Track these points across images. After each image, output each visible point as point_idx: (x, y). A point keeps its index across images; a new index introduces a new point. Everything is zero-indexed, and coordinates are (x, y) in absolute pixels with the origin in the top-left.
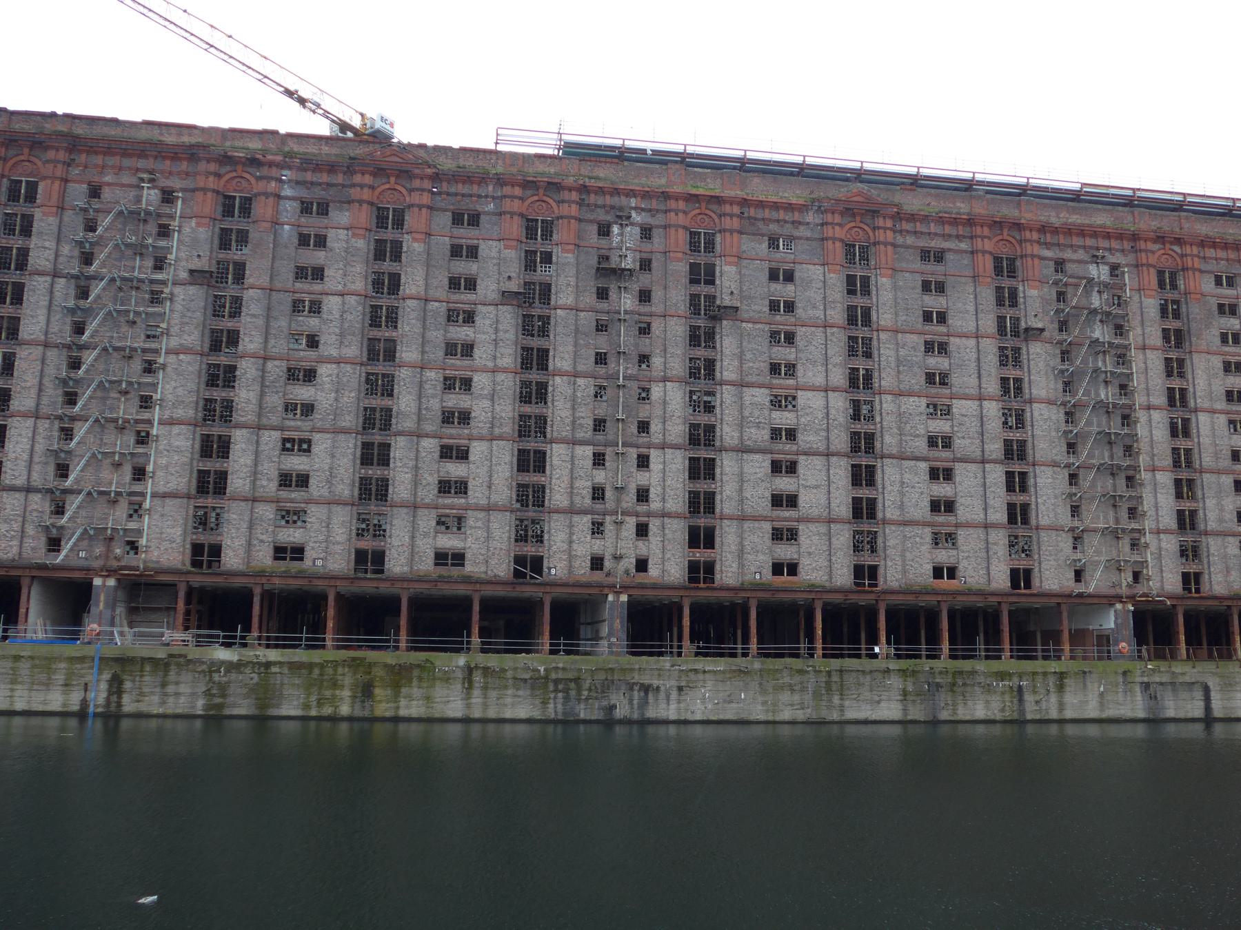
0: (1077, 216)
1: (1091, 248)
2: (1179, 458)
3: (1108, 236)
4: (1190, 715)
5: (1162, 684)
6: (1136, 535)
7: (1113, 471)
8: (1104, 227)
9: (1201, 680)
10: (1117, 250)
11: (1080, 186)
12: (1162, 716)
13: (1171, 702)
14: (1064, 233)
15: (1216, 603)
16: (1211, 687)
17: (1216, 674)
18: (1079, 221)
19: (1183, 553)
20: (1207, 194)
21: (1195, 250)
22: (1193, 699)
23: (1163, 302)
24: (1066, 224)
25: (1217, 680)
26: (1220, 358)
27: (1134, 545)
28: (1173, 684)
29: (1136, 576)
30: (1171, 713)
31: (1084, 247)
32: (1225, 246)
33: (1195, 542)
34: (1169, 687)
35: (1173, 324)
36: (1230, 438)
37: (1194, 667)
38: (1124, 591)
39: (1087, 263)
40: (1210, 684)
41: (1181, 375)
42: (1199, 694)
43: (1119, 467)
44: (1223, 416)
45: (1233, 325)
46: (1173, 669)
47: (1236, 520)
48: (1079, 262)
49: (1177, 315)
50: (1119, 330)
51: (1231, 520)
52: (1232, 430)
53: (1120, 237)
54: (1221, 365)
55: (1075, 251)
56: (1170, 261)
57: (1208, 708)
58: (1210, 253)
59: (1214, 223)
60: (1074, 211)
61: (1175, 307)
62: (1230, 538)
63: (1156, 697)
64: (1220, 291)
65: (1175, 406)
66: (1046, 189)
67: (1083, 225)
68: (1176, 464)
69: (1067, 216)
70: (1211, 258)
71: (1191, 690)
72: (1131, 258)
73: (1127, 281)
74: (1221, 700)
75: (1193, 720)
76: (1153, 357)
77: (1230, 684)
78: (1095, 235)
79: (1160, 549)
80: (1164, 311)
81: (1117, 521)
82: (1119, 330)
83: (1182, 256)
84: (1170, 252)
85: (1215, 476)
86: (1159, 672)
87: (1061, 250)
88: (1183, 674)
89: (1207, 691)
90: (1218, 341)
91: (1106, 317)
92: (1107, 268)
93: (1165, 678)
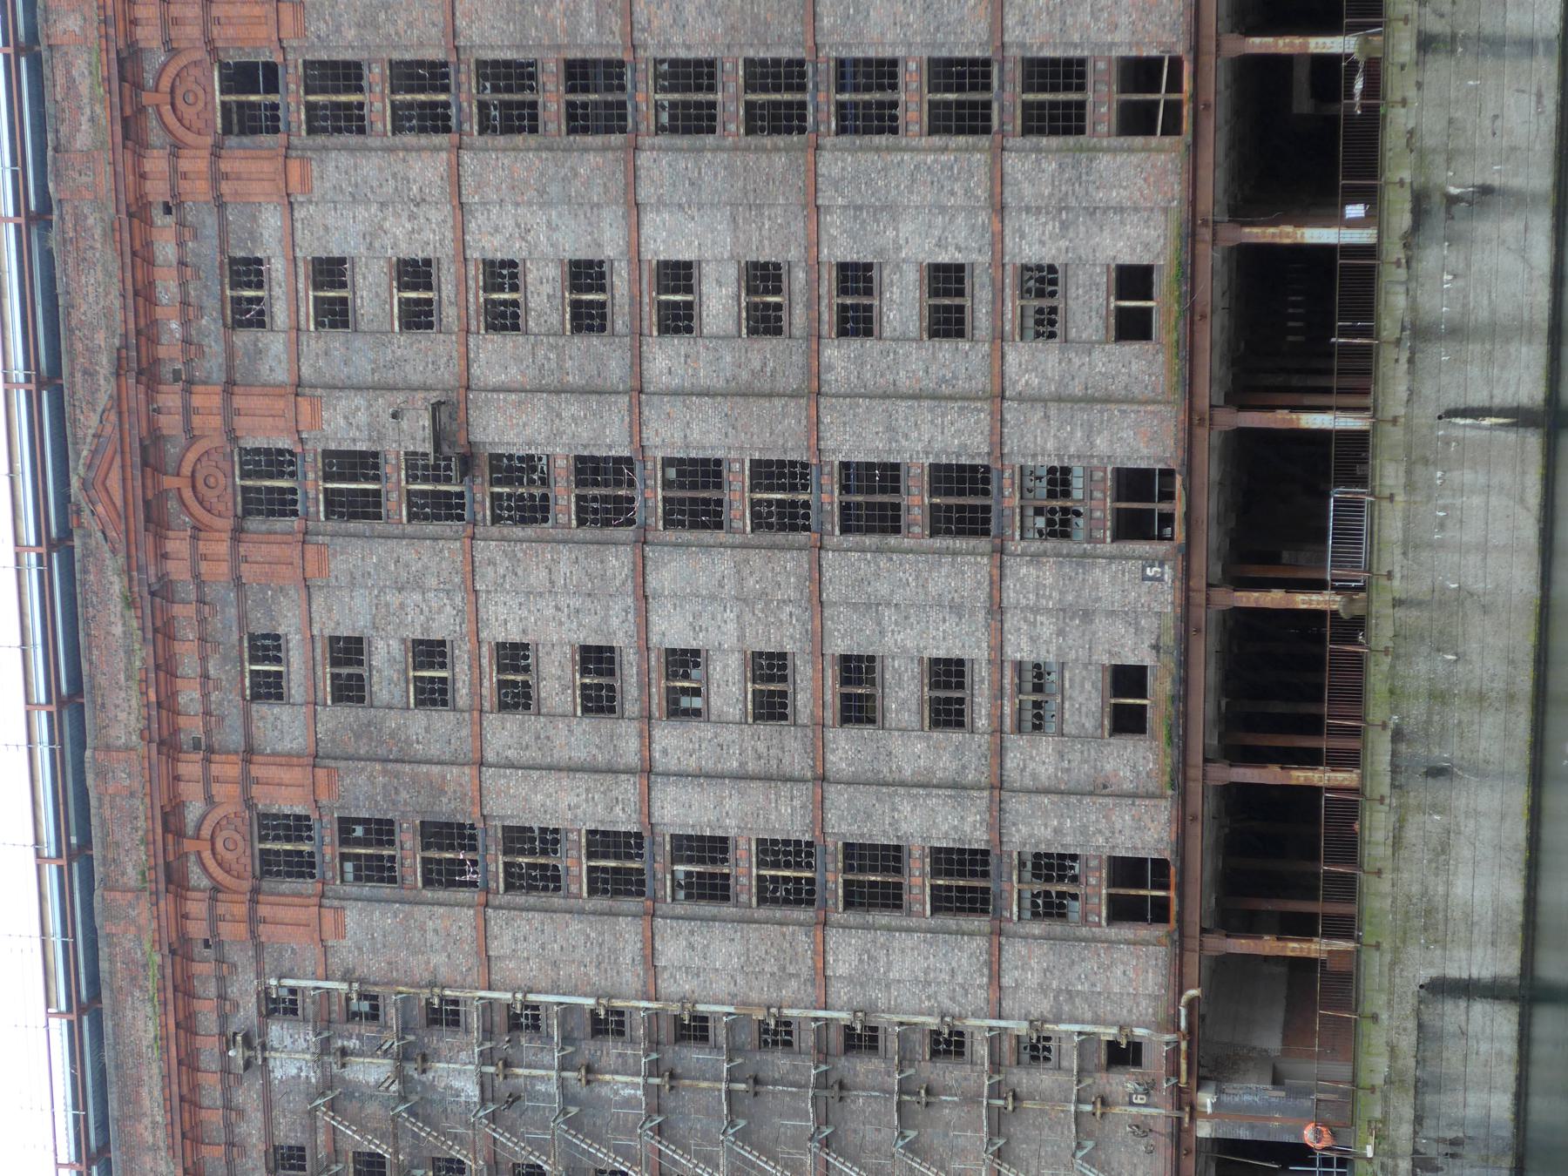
0: (144, 1092)
1: (226, 1070)
2: (786, 879)
3: (187, 1025)
4: (1510, 1049)
5: (1418, 1120)
6: (1007, 1046)
7: (834, 1089)
8: (162, 1039)
9: (1411, 1001)
10: (222, 997)
11: (54, 1022)
12: (1507, 1132)
13: (1472, 1098)
14: (198, 1141)
15: (1196, 830)
16: (1433, 973)
17: (1396, 950)
18: (157, 1093)
19: (1052, 908)
20: (16, 640)
21: (190, 767)
22: (1464, 1034)
23: (349, 866)
24: (171, 1148)
25: (1414, 951)
26: (492, 720)
27: (1038, 1050)
28: (1420, 1087)
29: (1124, 1055)
30: (1501, 1104)
31: (226, 1091)
32: (165, 668)
33: (1022, 864)
34: (1429, 1099)
35: (409, 852)
36: (722, 722)
37: (1375, 1018)
38: (1160, 1113)
39: (267, 1084)
40: (1425, 974)
41: (550, 839)
42: (1453, 1013)
43: (823, 1082)
44: (657, 733)
45: (392, 660)
46: (1379, 1080)
47: (956, 736)
48: (268, 1106)
49: (382, 830)
50: (445, 1016)
51: (959, 750)
52: (697, 703)
53: (183, 990)
54: (513, 721)
55: (241, 1113)
56: (225, 834)
57: (1491, 991)
58: (189, 696)
59: (102, 680)
60: (131, 1100)
61: (359, 831)
62: (1010, 764)
63: (1455, 1142)
64: (296, 686)
65: (640, 872)
66: (79, 1124)
67: (168, 1099)
68: (802, 895)
69: (146, 1121)
70: (207, 713)
71: (1439, 1037)
72: (240, 956)
73: (311, 983)
74: (1470, 947)
75: (1524, 1039)
76: (506, 938)
77: (1429, 912)
78: (188, 1062)
79: (1043, 989)
80: (379, 871)
81: (971, 1099)
82: (445, 1016)
83: (209, 800)
84: (206, 832)
85: (832, 791)
86: (1384, 1121)
87: (244, 1152)
88: (1393, 1050)
89: (1441, 988)
90: (442, 720)
91: (412, 1056)
92: (277, 1031)
93: (1404, 1108)
